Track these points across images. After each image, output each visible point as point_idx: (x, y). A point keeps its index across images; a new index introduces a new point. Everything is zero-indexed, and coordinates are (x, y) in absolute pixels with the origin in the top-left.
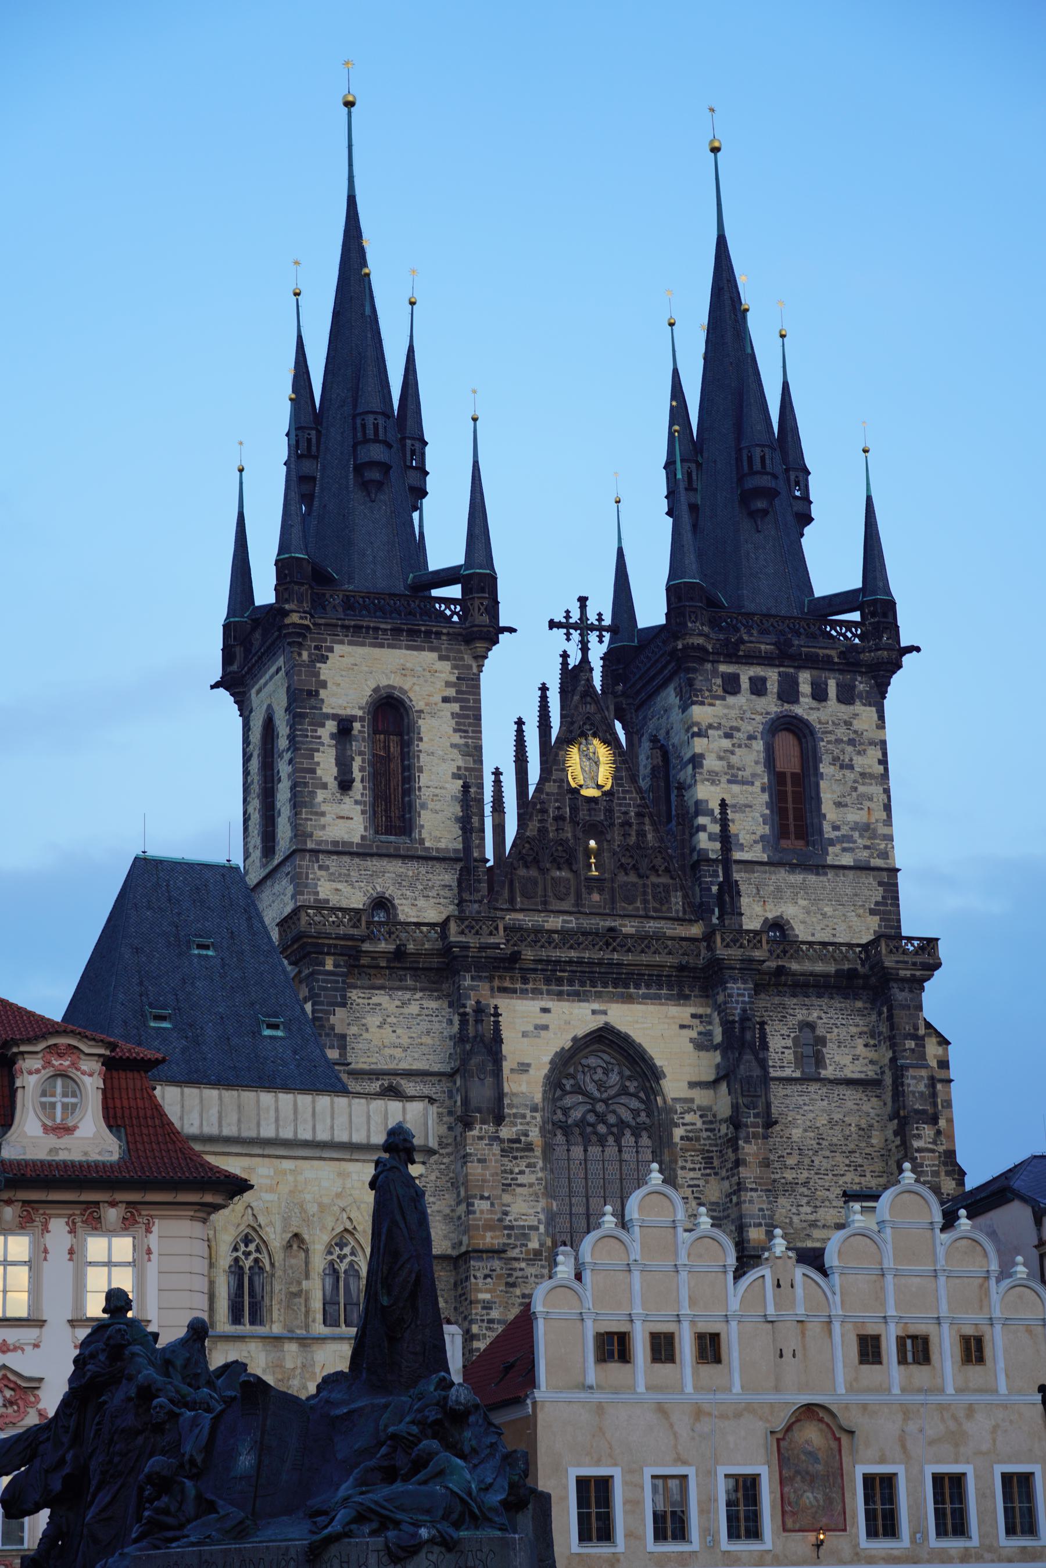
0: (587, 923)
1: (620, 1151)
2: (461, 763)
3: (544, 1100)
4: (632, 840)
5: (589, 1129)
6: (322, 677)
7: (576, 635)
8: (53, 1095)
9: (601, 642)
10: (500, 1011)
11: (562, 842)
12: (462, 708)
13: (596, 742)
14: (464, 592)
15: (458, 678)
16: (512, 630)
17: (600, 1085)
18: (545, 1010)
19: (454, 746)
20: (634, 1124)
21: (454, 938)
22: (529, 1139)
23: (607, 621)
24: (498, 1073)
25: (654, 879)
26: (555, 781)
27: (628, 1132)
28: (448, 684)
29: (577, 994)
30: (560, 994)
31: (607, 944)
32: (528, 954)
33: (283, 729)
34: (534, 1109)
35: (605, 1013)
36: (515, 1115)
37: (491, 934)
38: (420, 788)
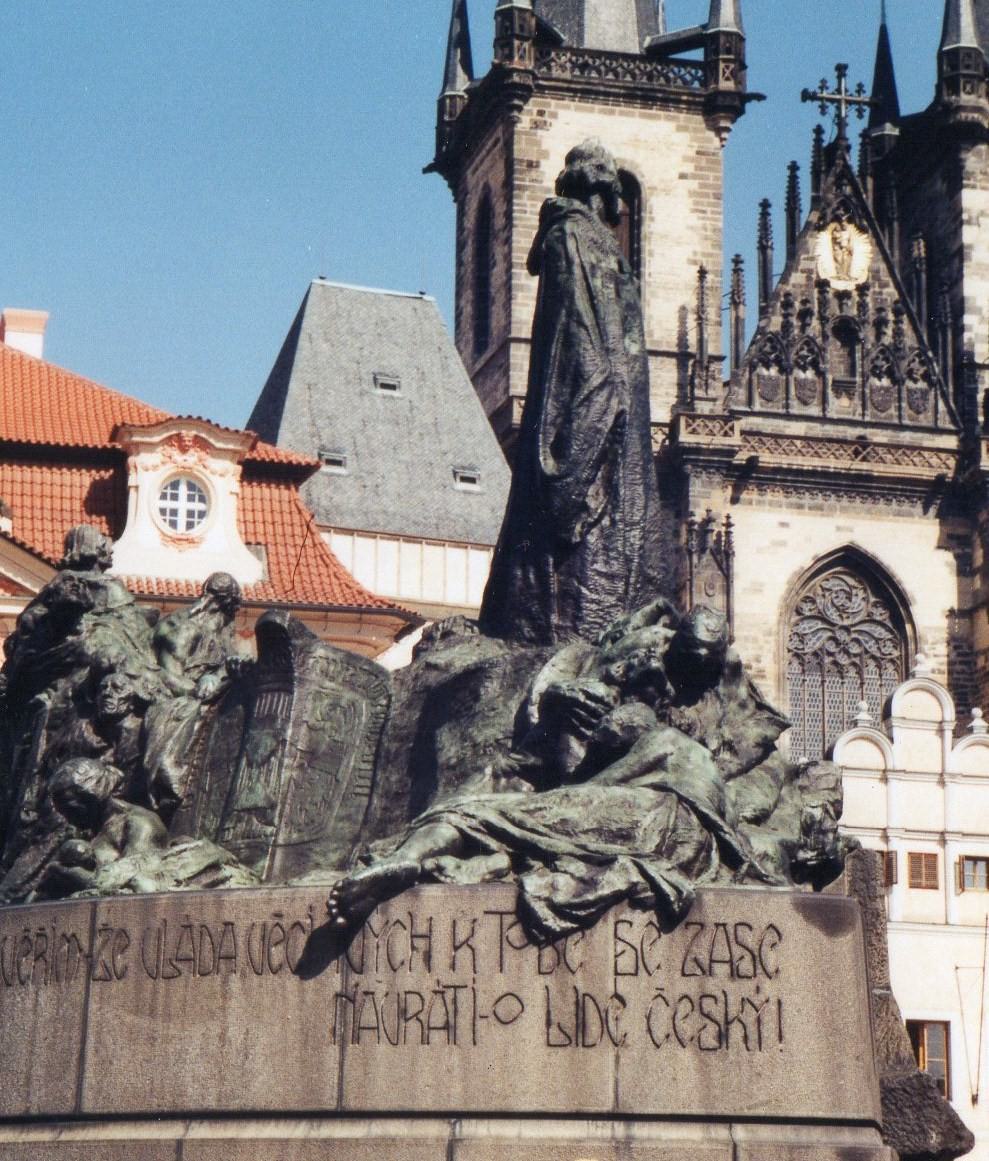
0: (831, 430)
1: (862, 684)
2: (699, 249)
3: (779, 623)
4: (887, 340)
5: (828, 660)
6: (544, 147)
7: (832, 109)
8: (175, 497)
9: (860, 116)
10: (732, 521)
11: (809, 342)
12: (702, 186)
13: (851, 229)
14: (706, 55)
15: (698, 153)
16: (760, 97)
17: (842, 611)
18: (783, 525)
19: (692, 228)
20: (878, 655)
21: (685, 437)
22: (761, 665)
23: (867, 96)
24: (728, 591)
25: (910, 384)
26: (803, 271)
27: (872, 664)
28: (686, 159)
29: (820, 508)
30: (800, 507)
31: (857, 453)
32: (767, 459)
33: (500, 208)
34: (769, 634)
35: (851, 531)
36: (746, 639)
37: (726, 434)
38: (650, 274)
